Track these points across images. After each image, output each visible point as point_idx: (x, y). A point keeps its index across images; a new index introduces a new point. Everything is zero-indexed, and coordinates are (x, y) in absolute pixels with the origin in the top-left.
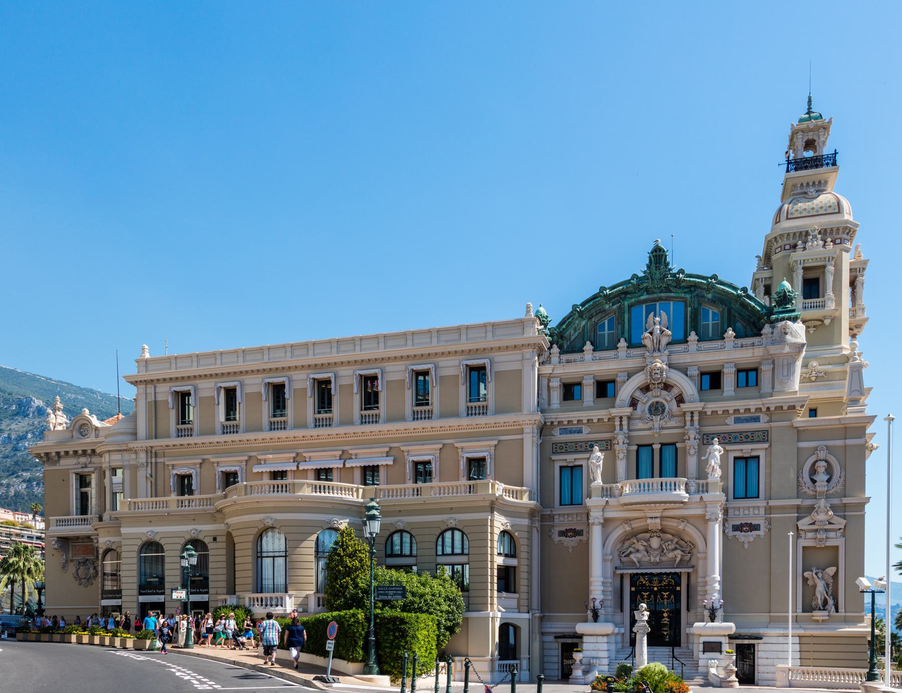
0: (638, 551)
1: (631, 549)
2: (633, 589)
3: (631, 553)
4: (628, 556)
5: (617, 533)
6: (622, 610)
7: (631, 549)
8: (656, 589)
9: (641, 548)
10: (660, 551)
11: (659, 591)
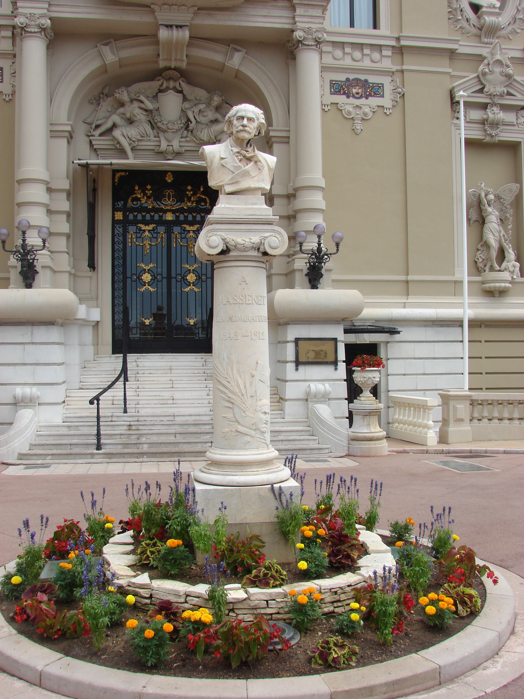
0: (130, 122)
1: (116, 118)
2: (119, 216)
3: (114, 126)
4: (110, 131)
5: (83, 66)
6: (92, 265)
7: (116, 118)
8: (169, 217)
9: (140, 116)
10: (179, 125)
11: (177, 222)
